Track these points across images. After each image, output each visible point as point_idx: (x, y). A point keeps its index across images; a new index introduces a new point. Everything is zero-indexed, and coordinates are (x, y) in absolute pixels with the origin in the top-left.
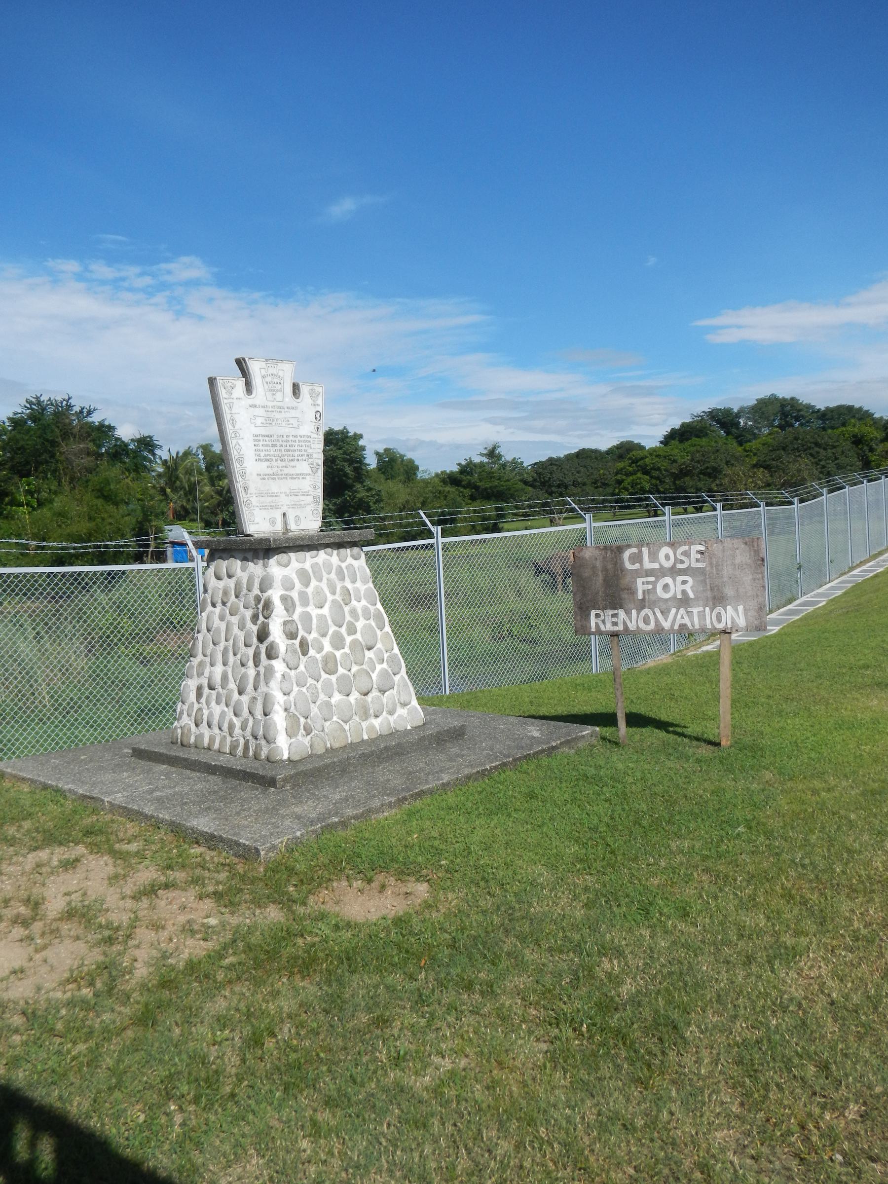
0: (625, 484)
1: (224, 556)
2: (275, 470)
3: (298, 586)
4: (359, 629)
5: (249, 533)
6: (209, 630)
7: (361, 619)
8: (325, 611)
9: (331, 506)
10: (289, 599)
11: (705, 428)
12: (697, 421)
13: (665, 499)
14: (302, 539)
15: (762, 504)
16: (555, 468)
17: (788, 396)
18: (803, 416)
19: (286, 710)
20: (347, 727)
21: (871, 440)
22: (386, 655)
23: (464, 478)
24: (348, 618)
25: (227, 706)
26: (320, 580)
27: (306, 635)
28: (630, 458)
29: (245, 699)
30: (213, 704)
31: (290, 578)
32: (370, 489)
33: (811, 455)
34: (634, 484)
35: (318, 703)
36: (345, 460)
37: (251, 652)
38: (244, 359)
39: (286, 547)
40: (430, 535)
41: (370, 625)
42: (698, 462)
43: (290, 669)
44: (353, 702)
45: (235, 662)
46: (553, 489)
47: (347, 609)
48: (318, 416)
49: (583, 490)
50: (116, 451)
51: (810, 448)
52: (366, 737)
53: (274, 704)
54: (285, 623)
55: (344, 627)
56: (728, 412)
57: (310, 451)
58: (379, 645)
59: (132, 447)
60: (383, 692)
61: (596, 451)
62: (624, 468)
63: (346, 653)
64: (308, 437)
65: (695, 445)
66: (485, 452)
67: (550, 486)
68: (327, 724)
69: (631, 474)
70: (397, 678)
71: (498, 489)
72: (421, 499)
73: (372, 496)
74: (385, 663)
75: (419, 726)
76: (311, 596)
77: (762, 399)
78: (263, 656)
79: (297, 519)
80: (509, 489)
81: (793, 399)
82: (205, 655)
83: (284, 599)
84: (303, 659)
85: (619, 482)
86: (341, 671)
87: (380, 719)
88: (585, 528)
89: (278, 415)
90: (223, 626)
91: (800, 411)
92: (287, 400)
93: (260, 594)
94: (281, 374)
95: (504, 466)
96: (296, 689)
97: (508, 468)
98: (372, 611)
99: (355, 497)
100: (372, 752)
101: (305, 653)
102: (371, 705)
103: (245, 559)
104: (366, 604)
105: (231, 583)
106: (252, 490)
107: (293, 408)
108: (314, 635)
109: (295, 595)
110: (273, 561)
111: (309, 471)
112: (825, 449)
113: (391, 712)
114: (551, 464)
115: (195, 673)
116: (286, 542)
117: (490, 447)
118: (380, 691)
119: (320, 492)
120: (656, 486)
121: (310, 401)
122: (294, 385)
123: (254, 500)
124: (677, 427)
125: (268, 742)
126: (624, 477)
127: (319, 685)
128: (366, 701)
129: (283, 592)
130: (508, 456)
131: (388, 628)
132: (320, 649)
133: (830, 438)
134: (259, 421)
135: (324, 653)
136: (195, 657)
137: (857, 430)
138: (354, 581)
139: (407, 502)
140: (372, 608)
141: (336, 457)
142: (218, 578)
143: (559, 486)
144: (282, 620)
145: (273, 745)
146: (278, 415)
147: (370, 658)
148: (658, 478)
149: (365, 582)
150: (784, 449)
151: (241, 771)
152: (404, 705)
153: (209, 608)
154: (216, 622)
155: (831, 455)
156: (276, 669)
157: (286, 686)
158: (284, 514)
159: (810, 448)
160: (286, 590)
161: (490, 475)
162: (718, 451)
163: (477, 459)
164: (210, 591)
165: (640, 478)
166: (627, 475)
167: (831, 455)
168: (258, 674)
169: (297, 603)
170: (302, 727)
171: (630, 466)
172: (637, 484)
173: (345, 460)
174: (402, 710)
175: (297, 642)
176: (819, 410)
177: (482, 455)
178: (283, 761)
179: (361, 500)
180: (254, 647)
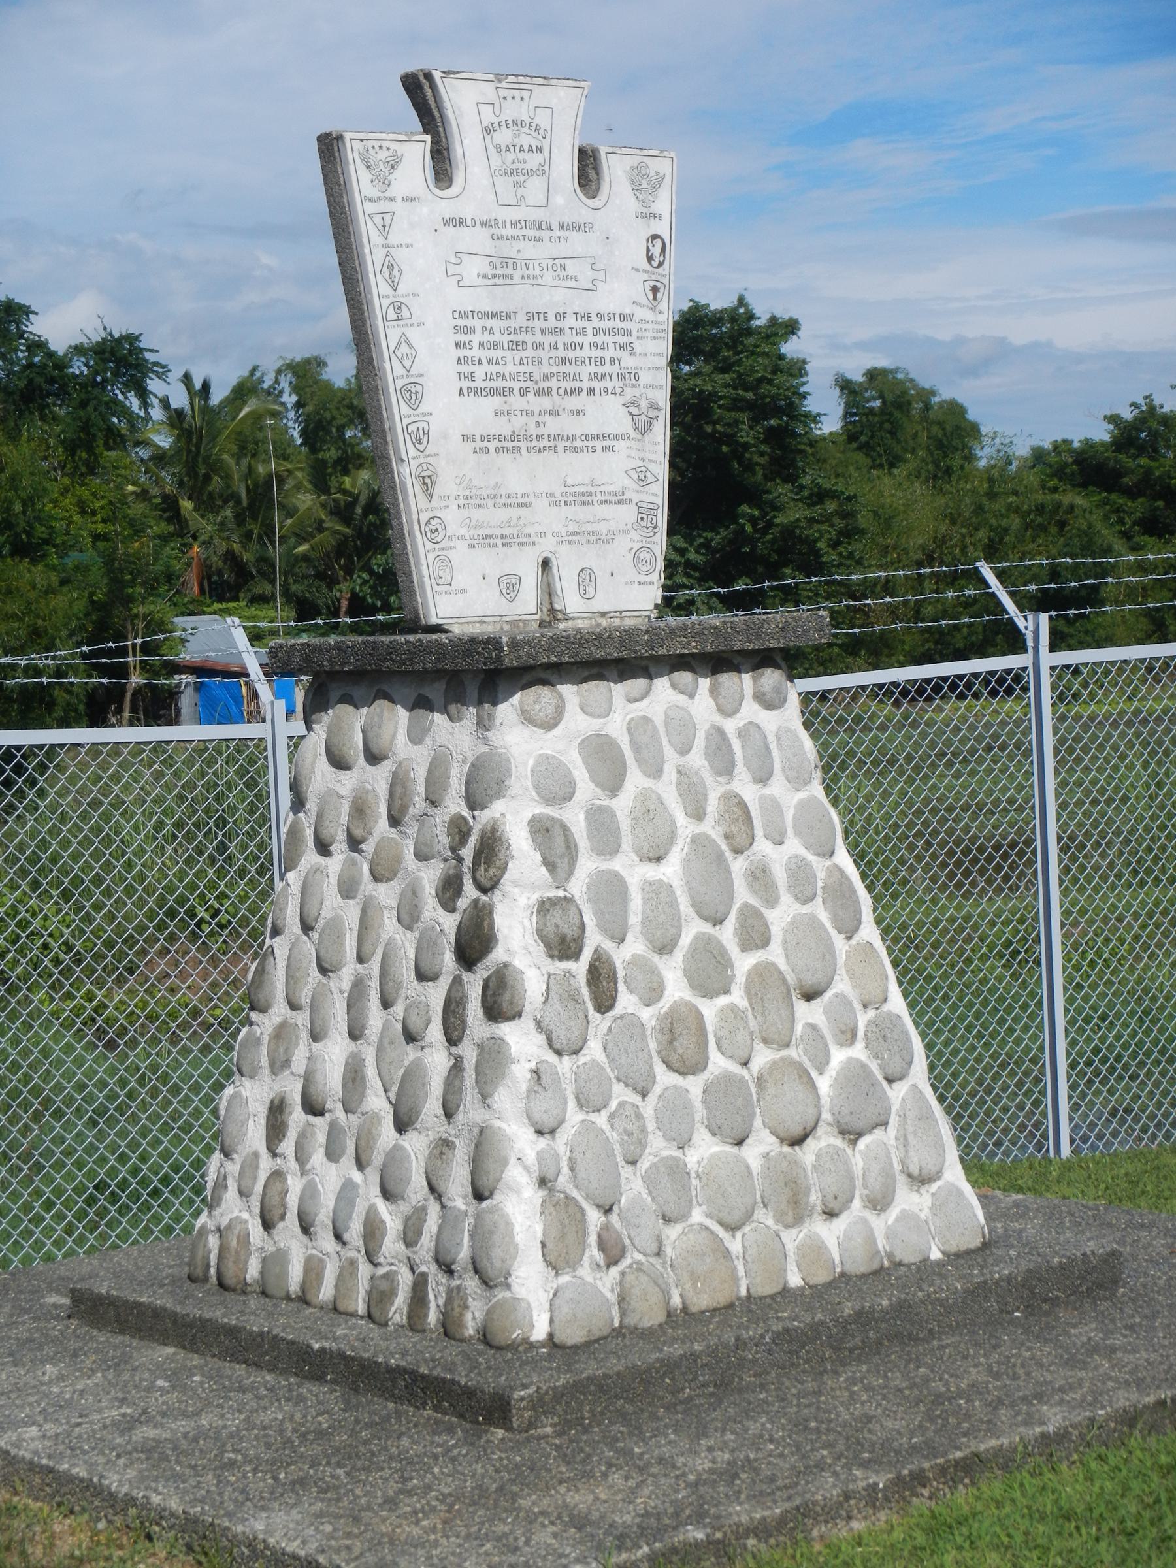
1: (358, 692)
2: (519, 422)
3: (586, 789)
4: (776, 931)
5: (434, 620)
6: (306, 927)
7: (786, 898)
8: (671, 870)
9: (692, 556)
10: (557, 831)
14: (600, 638)
19: (543, 1182)
20: (735, 1245)
22: (863, 1019)
23: (1131, 464)
24: (743, 894)
25: (361, 1165)
26: (656, 772)
27: (608, 946)
29: (416, 1145)
30: (318, 1157)
31: (561, 765)
32: (820, 496)
35: (644, 1164)
36: (737, 405)
37: (436, 995)
38: (428, 76)
39: (548, 666)
40: (1014, 642)
41: (813, 919)
43: (558, 1053)
44: (755, 1164)
45: (385, 1027)
47: (738, 866)
48: (656, 250)
50: (31, 381)
52: (795, 1280)
53: (505, 1163)
54: (544, 907)
55: (731, 924)
57: (629, 362)
58: (841, 985)
59: (78, 367)
60: (852, 1135)
63: (733, 1008)
64: (624, 317)
68: (672, 1233)
70: (897, 1093)
73: (827, 519)
74: (860, 1045)
75: (969, 1252)
76: (625, 824)
78: (474, 1010)
79: (587, 578)
82: (293, 1006)
83: (542, 830)
84: (600, 1023)
86: (718, 1063)
87: (841, 1224)
89: (530, 251)
90: (351, 913)
92: (559, 200)
93: (466, 813)
94: (542, 119)
96: (574, 1116)
98: (821, 875)
99: (770, 525)
100: (816, 1329)
101: (605, 1003)
102: (813, 1178)
103: (421, 703)
104: (803, 851)
105: (378, 779)
106: (446, 485)
107: (577, 227)
108: (634, 946)
109: (575, 817)
110: (507, 710)
111: (626, 426)
113: (879, 1203)
115: (264, 1062)
116: (551, 650)
118: (843, 1133)
119: (658, 494)
121: (633, 205)
122: (582, 152)
123: (452, 518)
125: (486, 1282)
127: (648, 1108)
128: (796, 1163)
129: (540, 809)
131: (869, 932)
132: (652, 994)
134: (473, 268)
135: (665, 1004)
136: (264, 1010)
138: (762, 778)
139: (941, 541)
140: (820, 867)
141: (713, 396)
142: (339, 762)
144: (535, 897)
145: (501, 1294)
146: (530, 251)
147: (813, 1027)
149: (798, 781)
151: (400, 1371)
152: (921, 1180)
153: (310, 857)
154: (331, 903)
156: (514, 1050)
157: (544, 1107)
158: (546, 564)
160: (550, 800)
164: (312, 805)
168: (457, 1067)
169: (583, 844)
170: (593, 1239)
173: (737, 405)
174: (914, 1198)
175: (580, 968)
178: (532, 1346)
179: (788, 532)
180: (444, 982)
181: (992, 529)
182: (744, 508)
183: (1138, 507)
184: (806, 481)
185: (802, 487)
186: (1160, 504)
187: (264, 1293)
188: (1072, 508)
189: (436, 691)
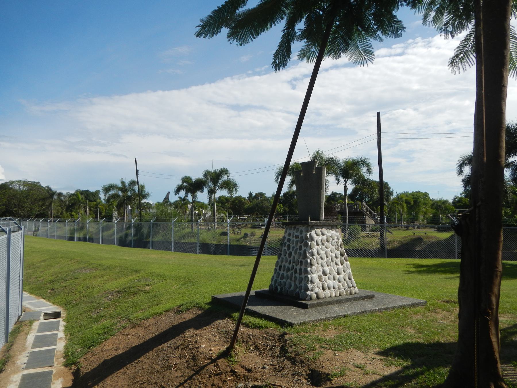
1: (319, 227)
6: (318, 254)
29: (341, 276)
30: (328, 280)
37: (339, 259)
82: (318, 264)
90: (324, 252)
142: (318, 235)
153: (316, 247)
180: (340, 258)
187: (325, 298)
189: (330, 228)
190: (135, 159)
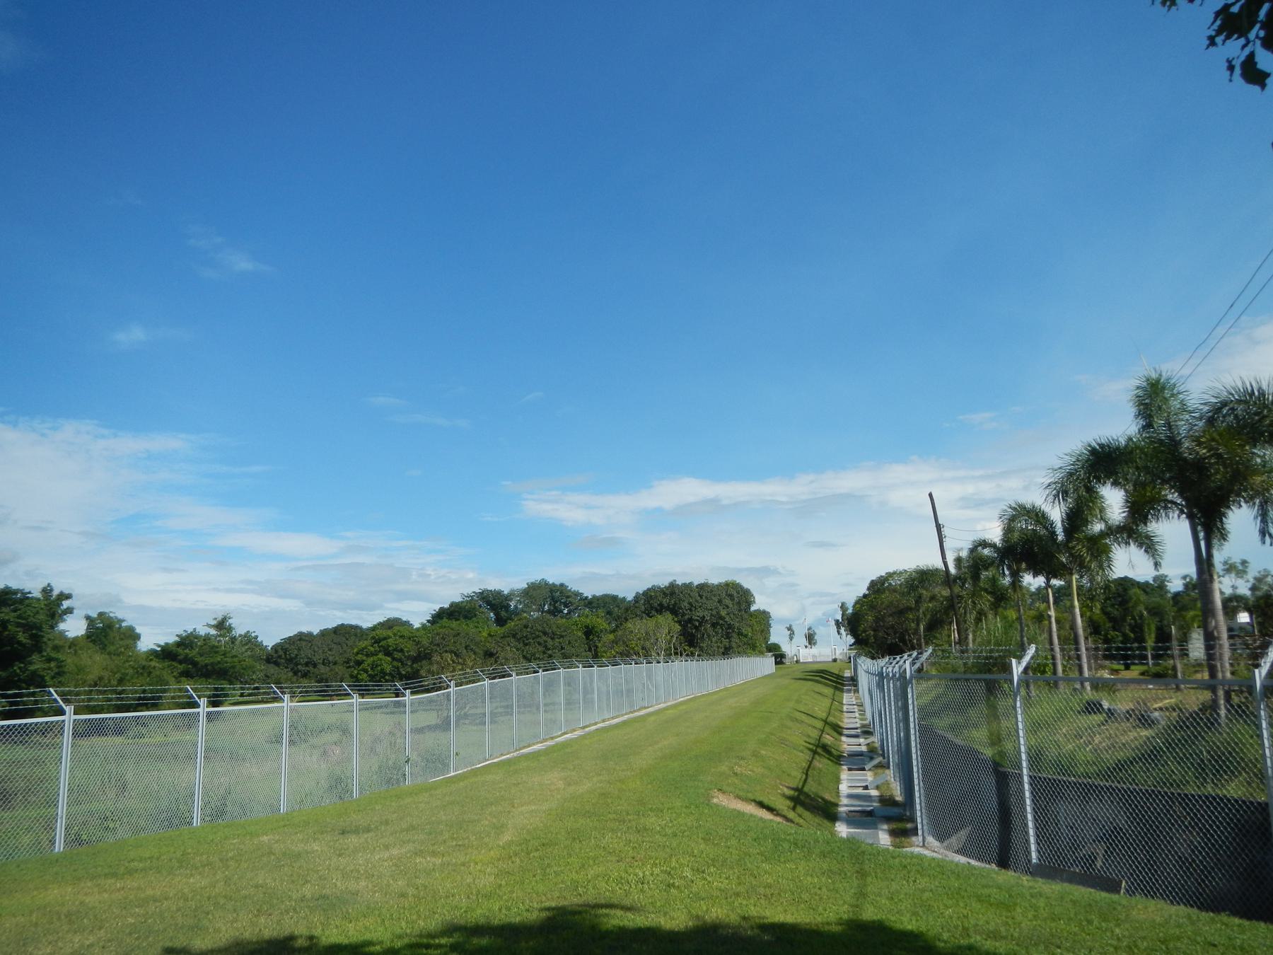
0: (364, 666)
11: (474, 608)
12: (467, 602)
13: (406, 684)
15: (355, 696)
16: (304, 643)
17: (557, 583)
18: (570, 602)
21: (601, 631)
28: (373, 638)
32: (49, 660)
33: (539, 644)
34: (373, 666)
36: (18, 625)
42: (438, 645)
46: (299, 667)
49: (331, 670)
51: (538, 636)
56: (498, 594)
61: (356, 627)
62: (366, 648)
65: (445, 627)
66: (214, 622)
67: (297, 664)
69: (373, 654)
71: (219, 666)
72: (118, 676)
77: (532, 583)
80: (233, 667)
81: (562, 585)
85: (359, 663)
88: (63, 721)
91: (568, 597)
95: (233, 640)
97: (237, 643)
99: (27, 670)
112: (553, 639)
114: (300, 640)
117: (220, 618)
120: (398, 668)
124: (446, 606)
126: (365, 658)
130: (240, 627)
133: (558, 627)
137: (588, 621)
139: (101, 678)
141: (8, 621)
143: (307, 664)
148: (400, 660)
150: (514, 636)
155: (557, 644)
159: (538, 636)
161: (214, 650)
162: (459, 634)
163: (203, 631)
165: (381, 660)
166: (367, 655)
167: (557, 644)
171: (372, 646)
172: (377, 666)
173: (18, 625)
176: (587, 597)
177: (208, 625)
179: (34, 673)
181: (122, 674)
182: (17, 663)
183: (181, 667)
184: (45, 654)
185: (43, 656)
186: (190, 666)
188: (154, 667)
190: (930, 495)
